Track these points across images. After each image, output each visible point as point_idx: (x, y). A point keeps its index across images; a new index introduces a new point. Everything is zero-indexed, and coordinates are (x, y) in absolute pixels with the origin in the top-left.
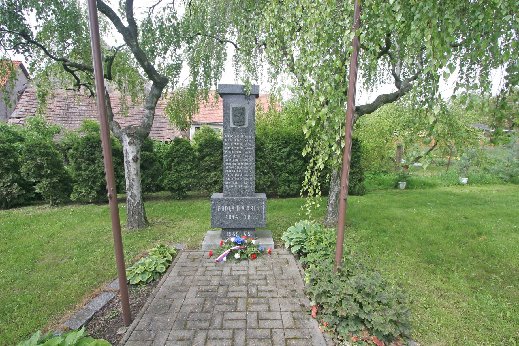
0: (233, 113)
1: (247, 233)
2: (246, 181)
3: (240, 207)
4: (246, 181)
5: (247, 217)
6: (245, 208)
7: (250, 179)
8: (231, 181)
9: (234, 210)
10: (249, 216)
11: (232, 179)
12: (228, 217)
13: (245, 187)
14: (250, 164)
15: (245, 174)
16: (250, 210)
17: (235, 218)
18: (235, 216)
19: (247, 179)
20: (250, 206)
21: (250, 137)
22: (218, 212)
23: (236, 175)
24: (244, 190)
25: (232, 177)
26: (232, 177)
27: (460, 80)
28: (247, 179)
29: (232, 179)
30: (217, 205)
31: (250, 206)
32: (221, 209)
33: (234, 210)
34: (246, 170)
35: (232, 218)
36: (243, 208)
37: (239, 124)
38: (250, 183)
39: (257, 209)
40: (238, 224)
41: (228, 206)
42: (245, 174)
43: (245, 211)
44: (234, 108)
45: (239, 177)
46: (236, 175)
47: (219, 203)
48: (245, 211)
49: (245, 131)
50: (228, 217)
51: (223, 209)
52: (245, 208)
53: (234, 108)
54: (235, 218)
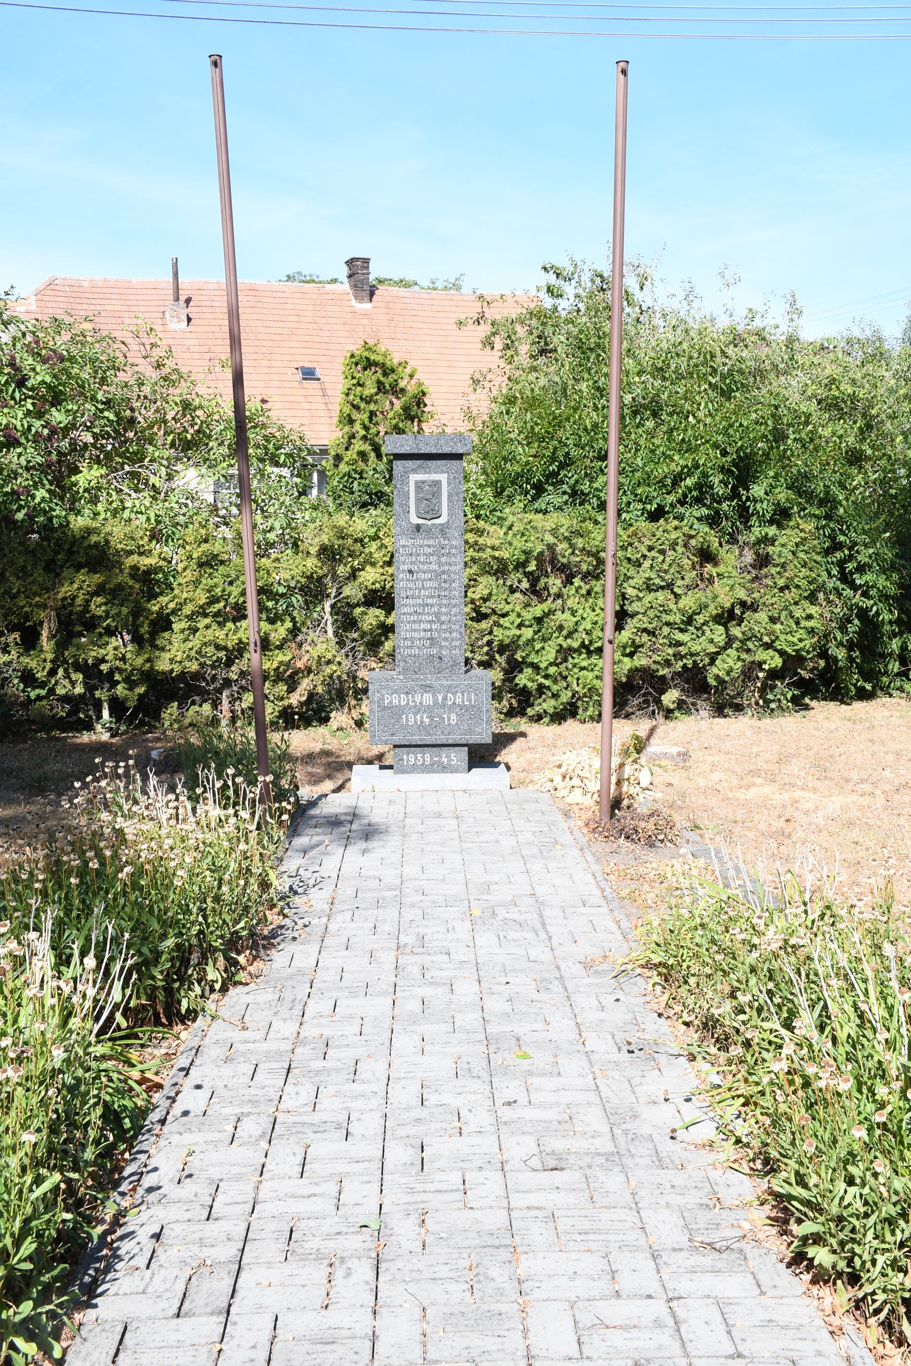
1: (448, 757)
2: (446, 639)
3: (434, 695)
4: (446, 639)
5: (449, 719)
6: (445, 698)
7: (454, 635)
8: (412, 639)
9: (421, 703)
10: (453, 716)
11: (416, 635)
12: (407, 720)
13: (444, 652)
14: (454, 602)
15: (443, 623)
16: (454, 703)
17: (422, 722)
19: (447, 635)
20: (454, 694)
21: (454, 543)
22: (385, 708)
23: (423, 626)
24: (440, 658)
25: (415, 630)
26: (415, 630)
28: (447, 635)
29: (416, 635)
31: (454, 694)
32: (391, 702)
33: (421, 703)
34: (446, 614)
35: (416, 722)
37: (429, 517)
38: (454, 643)
40: (430, 734)
41: (407, 693)
42: (443, 623)
43: (444, 705)
44: (416, 482)
45: (431, 630)
46: (423, 626)
47: (387, 687)
48: (444, 705)
49: (442, 530)
50: (407, 720)
51: (395, 702)
52: (445, 698)
53: (416, 482)
54: (422, 722)
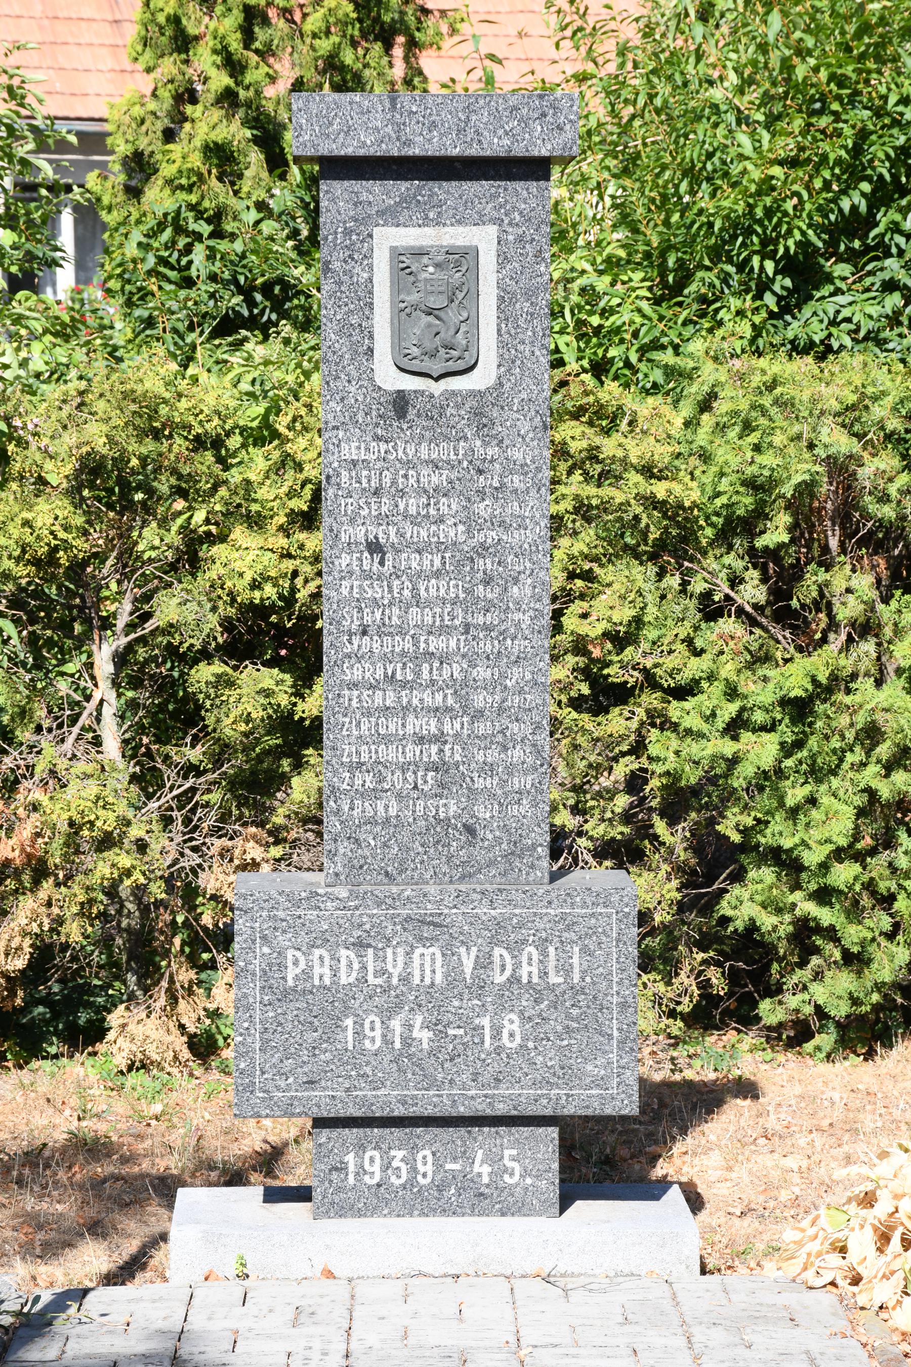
0: (397, 287)
1: (494, 1159)
2: (488, 769)
3: (448, 952)
4: (488, 769)
5: (497, 1034)
6: (484, 963)
7: (516, 754)
8: (378, 768)
9: (405, 979)
10: (512, 1023)
11: (390, 754)
12: (359, 1034)
13: (483, 812)
14: (515, 647)
15: (479, 714)
16: (514, 979)
17: (407, 1041)
18: (409, 1027)
19: (493, 755)
20: (516, 948)
21: (517, 454)
22: (286, 995)
23: (413, 724)
24: (470, 830)
25: (387, 740)
26: (387, 740)
27: (382, 563)
28: (493, 755)
29: (390, 754)
30: (282, 940)
31: (516, 948)
32: (307, 975)
33: (405, 979)
34: (490, 686)
35: (387, 1041)
36: (468, 965)
37: (436, 368)
38: (516, 782)
39: (567, 971)
40: (433, 1084)
41: (360, 945)
42: (479, 714)
43: (480, 987)
44: (397, 254)
45: (439, 738)
46: (413, 724)
47: (295, 925)
48: (480, 987)
49: (478, 413)
50: (359, 1034)
51: (322, 972)
52: (484, 963)
53: (397, 254)
54: (407, 1041)
